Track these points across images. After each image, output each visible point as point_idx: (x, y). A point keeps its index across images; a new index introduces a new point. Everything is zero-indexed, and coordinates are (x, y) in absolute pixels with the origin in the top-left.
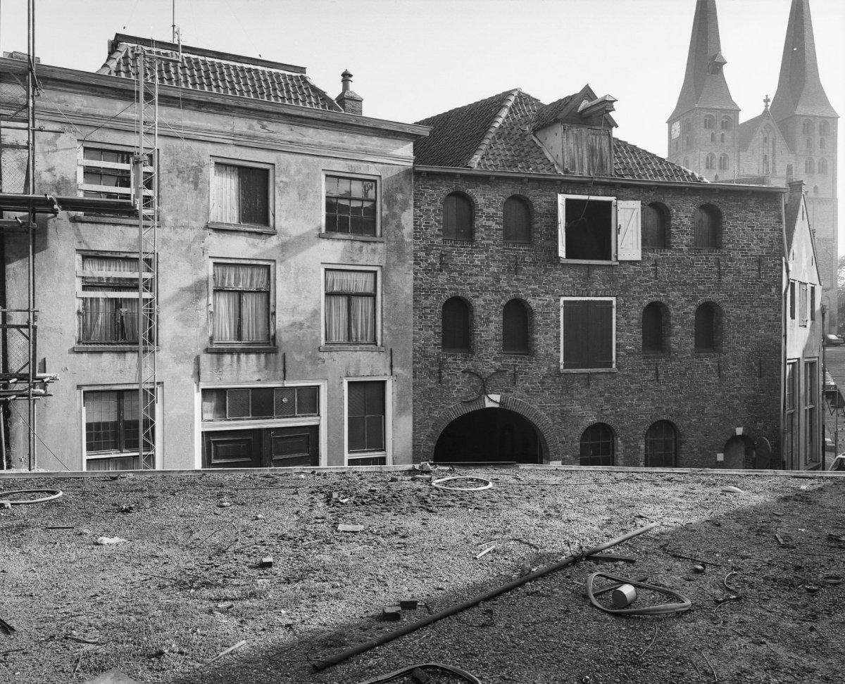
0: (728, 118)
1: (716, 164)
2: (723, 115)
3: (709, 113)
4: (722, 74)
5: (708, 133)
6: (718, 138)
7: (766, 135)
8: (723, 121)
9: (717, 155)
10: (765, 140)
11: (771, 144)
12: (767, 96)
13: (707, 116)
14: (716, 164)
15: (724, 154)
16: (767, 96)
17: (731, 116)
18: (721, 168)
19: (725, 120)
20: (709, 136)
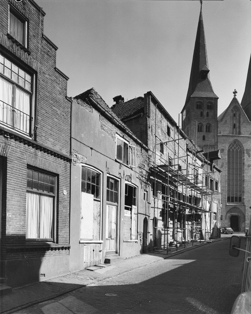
0: (211, 103)
1: (204, 128)
2: (208, 101)
3: (199, 100)
4: (208, 79)
5: (199, 112)
6: (205, 114)
7: (234, 112)
8: (208, 105)
9: (205, 124)
10: (235, 115)
11: (238, 117)
12: (235, 90)
13: (198, 102)
14: (204, 128)
15: (209, 124)
16: (235, 90)
17: (213, 101)
18: (206, 131)
19: (209, 104)
20: (199, 113)
